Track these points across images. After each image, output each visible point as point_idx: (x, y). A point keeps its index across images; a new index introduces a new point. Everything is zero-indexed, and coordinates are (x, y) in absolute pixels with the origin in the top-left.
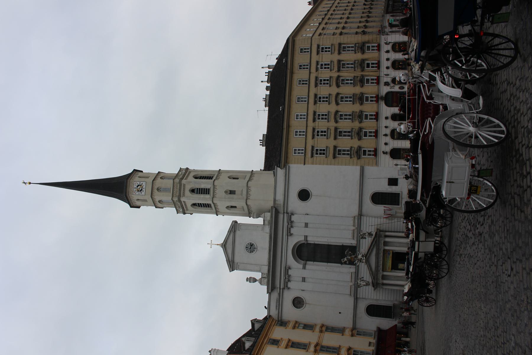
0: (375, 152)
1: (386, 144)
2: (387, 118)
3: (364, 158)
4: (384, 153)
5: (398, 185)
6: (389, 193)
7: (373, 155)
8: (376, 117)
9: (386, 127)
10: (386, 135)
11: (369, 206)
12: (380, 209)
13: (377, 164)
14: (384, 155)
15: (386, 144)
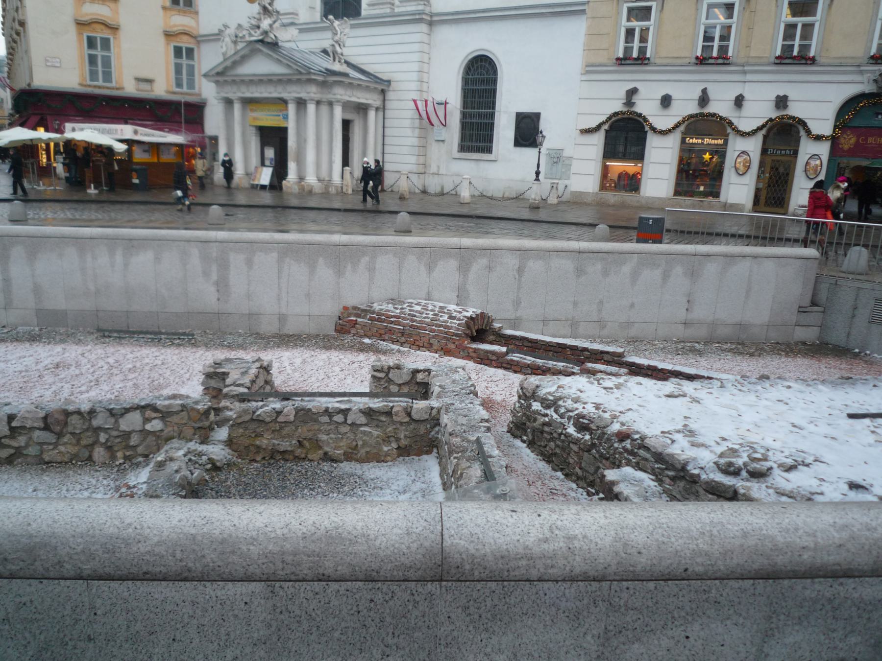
0: (635, 60)
1: (666, 101)
2: (782, 102)
3: (619, 13)
4: (632, 92)
5: (519, 149)
6: (492, 116)
7: (628, 50)
8: (795, 58)
9: (739, 101)
10: (704, 100)
11: (456, 48)
12: (449, 89)
13: (591, 69)
14: (622, 94)
15: (666, 101)
